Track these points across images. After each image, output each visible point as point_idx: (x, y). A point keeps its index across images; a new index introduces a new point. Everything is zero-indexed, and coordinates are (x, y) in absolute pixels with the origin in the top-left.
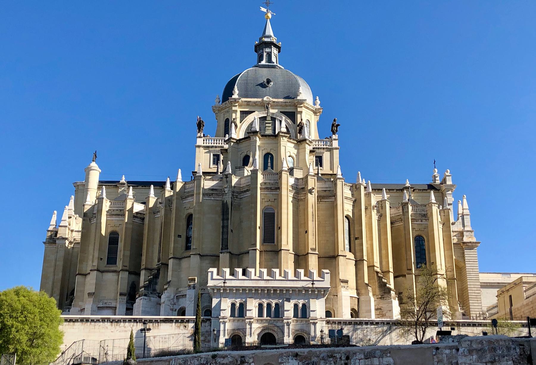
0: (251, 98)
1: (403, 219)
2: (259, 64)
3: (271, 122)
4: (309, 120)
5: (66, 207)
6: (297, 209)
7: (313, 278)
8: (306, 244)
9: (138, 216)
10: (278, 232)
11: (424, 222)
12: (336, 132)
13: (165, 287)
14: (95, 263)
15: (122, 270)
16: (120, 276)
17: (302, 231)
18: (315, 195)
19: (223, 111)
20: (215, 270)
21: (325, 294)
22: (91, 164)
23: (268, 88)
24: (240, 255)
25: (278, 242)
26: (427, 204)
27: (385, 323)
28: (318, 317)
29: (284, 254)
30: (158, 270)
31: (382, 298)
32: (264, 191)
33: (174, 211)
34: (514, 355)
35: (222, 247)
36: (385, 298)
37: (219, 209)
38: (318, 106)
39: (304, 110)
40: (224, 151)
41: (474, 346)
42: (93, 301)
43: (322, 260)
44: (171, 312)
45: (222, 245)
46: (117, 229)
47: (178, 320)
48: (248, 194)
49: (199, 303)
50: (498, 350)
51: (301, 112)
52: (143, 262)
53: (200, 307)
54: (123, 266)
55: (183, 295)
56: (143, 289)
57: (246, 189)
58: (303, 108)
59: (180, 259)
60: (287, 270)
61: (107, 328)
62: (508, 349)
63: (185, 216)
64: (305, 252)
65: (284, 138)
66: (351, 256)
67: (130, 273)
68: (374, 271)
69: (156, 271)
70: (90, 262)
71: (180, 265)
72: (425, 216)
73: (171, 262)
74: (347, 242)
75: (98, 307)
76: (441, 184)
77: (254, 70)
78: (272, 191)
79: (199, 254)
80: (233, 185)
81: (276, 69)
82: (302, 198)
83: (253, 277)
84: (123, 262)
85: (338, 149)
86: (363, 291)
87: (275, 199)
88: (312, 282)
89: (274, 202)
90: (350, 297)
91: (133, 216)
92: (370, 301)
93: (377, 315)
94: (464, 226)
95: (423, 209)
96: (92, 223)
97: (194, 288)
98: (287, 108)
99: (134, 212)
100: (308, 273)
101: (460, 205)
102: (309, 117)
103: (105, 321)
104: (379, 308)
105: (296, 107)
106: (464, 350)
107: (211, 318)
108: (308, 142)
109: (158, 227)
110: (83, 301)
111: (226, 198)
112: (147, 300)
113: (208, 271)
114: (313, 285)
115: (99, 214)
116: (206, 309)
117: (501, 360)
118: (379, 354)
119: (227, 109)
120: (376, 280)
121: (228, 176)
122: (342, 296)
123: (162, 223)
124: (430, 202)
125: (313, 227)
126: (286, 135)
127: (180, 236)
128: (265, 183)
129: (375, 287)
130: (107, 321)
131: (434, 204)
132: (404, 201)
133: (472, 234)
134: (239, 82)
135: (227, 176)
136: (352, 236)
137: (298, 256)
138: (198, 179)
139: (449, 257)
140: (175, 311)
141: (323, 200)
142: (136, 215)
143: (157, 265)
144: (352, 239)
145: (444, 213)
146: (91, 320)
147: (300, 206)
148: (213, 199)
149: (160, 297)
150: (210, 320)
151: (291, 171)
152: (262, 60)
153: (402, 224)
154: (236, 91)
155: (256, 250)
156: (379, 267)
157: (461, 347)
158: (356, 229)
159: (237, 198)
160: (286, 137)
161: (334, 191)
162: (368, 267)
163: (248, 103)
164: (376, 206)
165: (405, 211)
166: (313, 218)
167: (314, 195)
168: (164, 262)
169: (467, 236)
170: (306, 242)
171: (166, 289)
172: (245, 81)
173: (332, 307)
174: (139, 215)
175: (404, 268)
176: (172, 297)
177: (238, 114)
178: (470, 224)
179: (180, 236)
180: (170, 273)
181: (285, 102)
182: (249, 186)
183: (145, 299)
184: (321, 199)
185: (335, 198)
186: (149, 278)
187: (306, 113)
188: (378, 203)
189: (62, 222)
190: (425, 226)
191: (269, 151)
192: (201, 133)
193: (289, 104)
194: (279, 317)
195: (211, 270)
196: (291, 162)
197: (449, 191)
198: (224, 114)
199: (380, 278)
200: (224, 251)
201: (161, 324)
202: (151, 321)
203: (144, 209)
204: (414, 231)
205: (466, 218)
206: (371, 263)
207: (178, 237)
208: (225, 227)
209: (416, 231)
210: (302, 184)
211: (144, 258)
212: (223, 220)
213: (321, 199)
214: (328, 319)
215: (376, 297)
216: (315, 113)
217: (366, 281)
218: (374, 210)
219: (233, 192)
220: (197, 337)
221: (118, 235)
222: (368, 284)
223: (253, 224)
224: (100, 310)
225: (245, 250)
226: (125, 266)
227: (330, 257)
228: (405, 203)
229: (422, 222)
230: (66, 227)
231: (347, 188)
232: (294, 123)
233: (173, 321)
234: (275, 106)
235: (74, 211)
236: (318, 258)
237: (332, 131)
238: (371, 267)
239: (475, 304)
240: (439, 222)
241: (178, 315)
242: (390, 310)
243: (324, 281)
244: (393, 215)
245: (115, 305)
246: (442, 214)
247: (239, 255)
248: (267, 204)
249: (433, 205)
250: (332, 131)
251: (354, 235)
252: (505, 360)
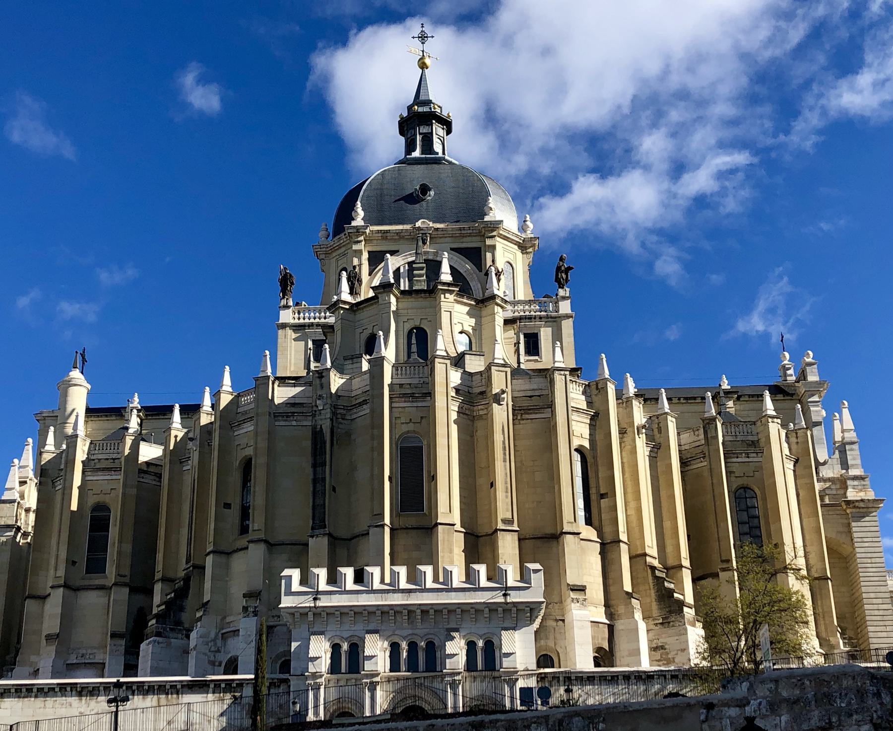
0: (391, 224)
1: (707, 454)
2: (408, 156)
3: (425, 265)
4: (512, 262)
5: (16, 461)
6: (472, 436)
7: (506, 582)
8: (493, 512)
9: (149, 470)
10: (430, 487)
11: (753, 458)
12: (567, 282)
13: (198, 615)
14: (61, 572)
15: (115, 584)
16: (112, 599)
17: (482, 481)
18: (507, 405)
19: (334, 254)
20: (295, 574)
21: (534, 618)
22: (71, 373)
23: (424, 203)
24: (353, 541)
25: (430, 508)
26: (757, 421)
27: (668, 677)
28: (520, 667)
29: (444, 532)
30: (187, 579)
31: (666, 623)
33: (216, 454)
34: (874, 709)
35: (313, 523)
36: (672, 623)
37: (308, 444)
38: (529, 234)
39: (500, 244)
40: (328, 329)
41: (785, 694)
42: (56, 651)
43: (528, 544)
44: (210, 667)
45: (313, 519)
46: (107, 499)
47: (220, 684)
48: (366, 409)
49: (261, 644)
50: (838, 701)
51: (493, 248)
52: (159, 567)
53: (265, 653)
54: (118, 575)
55: (234, 631)
56: (154, 621)
57: (361, 400)
58: (498, 239)
59: (229, 554)
60: (449, 568)
61: (71, 705)
62: (861, 694)
63: (238, 462)
64: (491, 527)
65: (447, 295)
66: (590, 533)
67: (133, 590)
68: (646, 566)
69: (182, 583)
70: (52, 572)
71: (227, 567)
72: (754, 444)
73: (209, 560)
74: (580, 503)
75: (67, 664)
76: (797, 381)
77: (397, 169)
78: (416, 401)
79: (266, 542)
80: (333, 391)
81: (441, 166)
82: (481, 413)
83: (377, 585)
84: (118, 567)
85: (572, 317)
86: (621, 609)
87: (421, 417)
88: (504, 592)
89: (420, 423)
90: (591, 622)
91: (139, 469)
92: (636, 630)
93: (656, 661)
94: (845, 465)
95: (749, 431)
96: (57, 489)
97: (255, 614)
98: (465, 239)
99: (139, 462)
100: (496, 574)
101: (837, 424)
102: (511, 256)
103: (66, 691)
104: (660, 644)
105: (483, 237)
106: (760, 704)
107: (289, 678)
108: (498, 301)
109: (187, 491)
110: (38, 654)
111: (321, 419)
112: (161, 645)
113: (282, 575)
114: (506, 599)
115: (68, 469)
116: (283, 659)
117: (846, 724)
118: (579, 724)
119: (343, 249)
120: (651, 585)
121: (324, 374)
122: (573, 620)
123: (194, 480)
124: (764, 414)
125: (506, 474)
126: (450, 288)
127: (227, 506)
128: (401, 385)
129: (648, 600)
130: (71, 691)
131: (773, 417)
132: (706, 415)
133: (864, 483)
134: (366, 194)
135: (322, 373)
136: (593, 491)
137: (478, 537)
138: (262, 384)
139: (809, 532)
140: (220, 665)
141: (527, 416)
142: (145, 469)
143: (184, 570)
144: (594, 497)
145: (797, 437)
146: (38, 688)
147: (477, 431)
148: (294, 423)
149: (188, 637)
150: (287, 681)
151: (458, 361)
152: (414, 150)
153: (705, 463)
154: (360, 212)
155: (383, 526)
156: (656, 556)
157: (753, 697)
158: (600, 476)
159: (343, 419)
160: (451, 292)
161: (550, 395)
162: (631, 558)
163: (385, 235)
164: (644, 427)
165: (709, 436)
166: (505, 454)
167: (505, 407)
168: (198, 562)
169: (854, 487)
170: (493, 507)
171: (200, 619)
172: (378, 192)
173: (553, 646)
174: (152, 469)
175: (716, 557)
176: (212, 635)
177: (365, 256)
178: (859, 462)
179: (227, 506)
180: (208, 585)
181: (460, 229)
182: (367, 393)
183: (158, 643)
184: (522, 414)
185: (552, 412)
186: (169, 597)
187: (505, 250)
188: (652, 421)
189: (6, 493)
190: (755, 467)
191: (417, 323)
192: (287, 299)
193: (469, 232)
194: (436, 671)
195: (286, 572)
196: (464, 344)
197: (813, 395)
198: (337, 261)
199: (659, 581)
200: (317, 532)
201: (184, 695)
202: (163, 688)
203: (161, 456)
204: (733, 479)
205: (849, 450)
206: (640, 549)
207: (224, 508)
208: (318, 481)
209: (736, 477)
210: (479, 385)
211: (160, 556)
212: (314, 466)
213: (522, 414)
214: (542, 671)
215: (653, 623)
216: (523, 247)
217: (628, 587)
218: (640, 436)
219: (335, 408)
220: (258, 718)
221: (108, 510)
222: (632, 593)
223: (376, 472)
224: (71, 670)
226: (121, 576)
227: (546, 538)
228: (710, 419)
229: (748, 457)
230: (13, 501)
231: (578, 388)
232: (481, 271)
233: (209, 686)
234: (440, 238)
235: (33, 470)
236: (520, 540)
237: (557, 280)
238: (638, 557)
239: (880, 635)
240: (784, 457)
241: (225, 674)
242: (685, 649)
243: (528, 588)
244: (687, 447)
245: (103, 660)
246: (793, 440)
247: (351, 539)
248: (405, 428)
249: (770, 420)
250: (556, 281)
251: (598, 487)
252: (854, 722)
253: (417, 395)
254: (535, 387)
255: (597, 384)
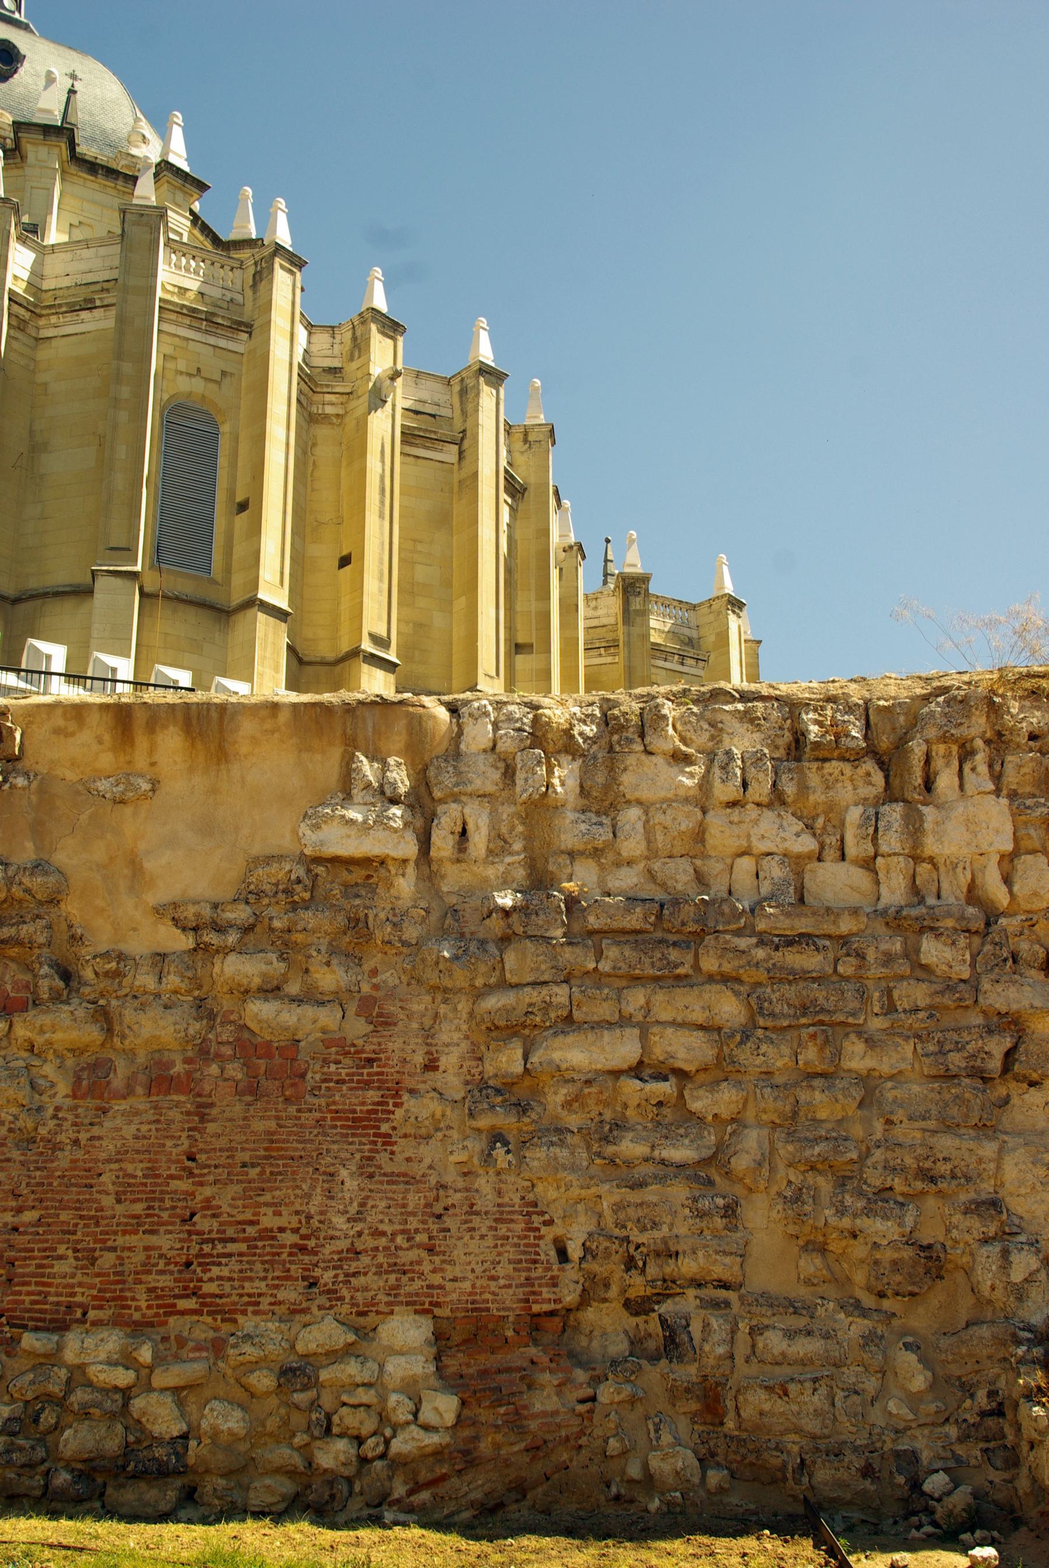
32: (178, 324)
82: (329, 410)
87: (224, 373)
165: (633, 608)
166: (382, 502)
225: (61, 576)
247: (17, 601)
248: (184, 385)
253: (220, 321)
254: (425, 395)
255: (526, 434)
